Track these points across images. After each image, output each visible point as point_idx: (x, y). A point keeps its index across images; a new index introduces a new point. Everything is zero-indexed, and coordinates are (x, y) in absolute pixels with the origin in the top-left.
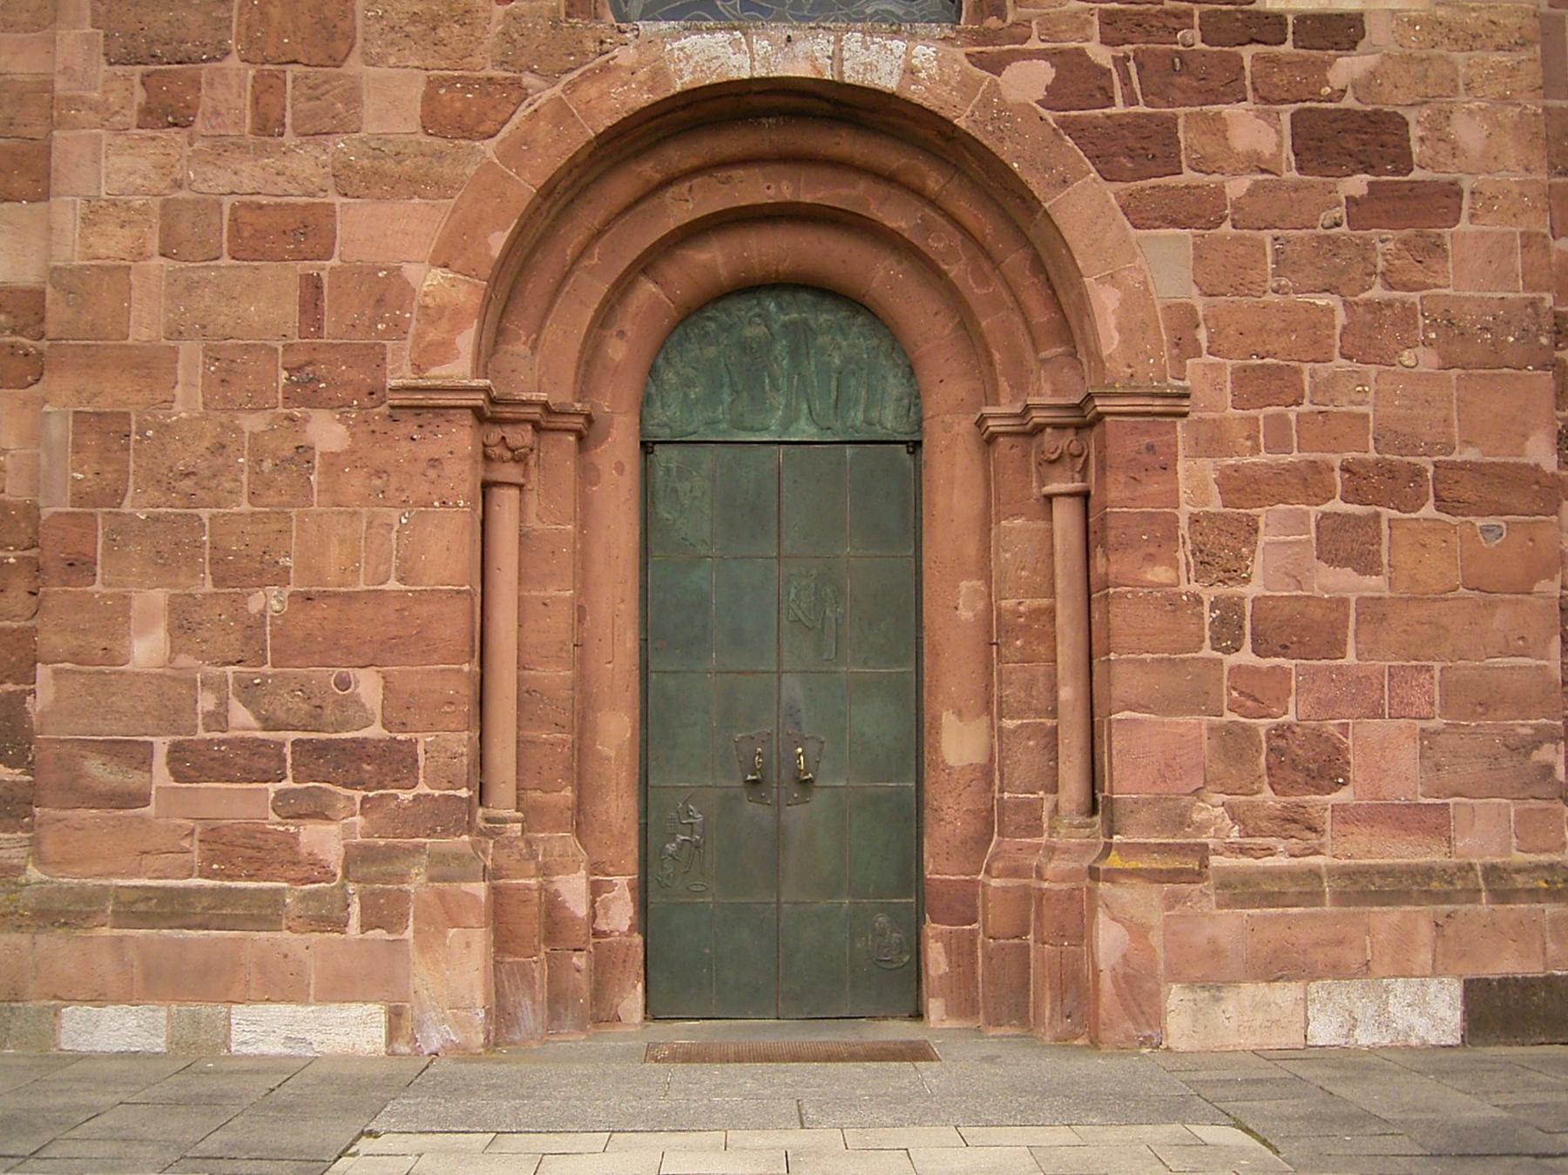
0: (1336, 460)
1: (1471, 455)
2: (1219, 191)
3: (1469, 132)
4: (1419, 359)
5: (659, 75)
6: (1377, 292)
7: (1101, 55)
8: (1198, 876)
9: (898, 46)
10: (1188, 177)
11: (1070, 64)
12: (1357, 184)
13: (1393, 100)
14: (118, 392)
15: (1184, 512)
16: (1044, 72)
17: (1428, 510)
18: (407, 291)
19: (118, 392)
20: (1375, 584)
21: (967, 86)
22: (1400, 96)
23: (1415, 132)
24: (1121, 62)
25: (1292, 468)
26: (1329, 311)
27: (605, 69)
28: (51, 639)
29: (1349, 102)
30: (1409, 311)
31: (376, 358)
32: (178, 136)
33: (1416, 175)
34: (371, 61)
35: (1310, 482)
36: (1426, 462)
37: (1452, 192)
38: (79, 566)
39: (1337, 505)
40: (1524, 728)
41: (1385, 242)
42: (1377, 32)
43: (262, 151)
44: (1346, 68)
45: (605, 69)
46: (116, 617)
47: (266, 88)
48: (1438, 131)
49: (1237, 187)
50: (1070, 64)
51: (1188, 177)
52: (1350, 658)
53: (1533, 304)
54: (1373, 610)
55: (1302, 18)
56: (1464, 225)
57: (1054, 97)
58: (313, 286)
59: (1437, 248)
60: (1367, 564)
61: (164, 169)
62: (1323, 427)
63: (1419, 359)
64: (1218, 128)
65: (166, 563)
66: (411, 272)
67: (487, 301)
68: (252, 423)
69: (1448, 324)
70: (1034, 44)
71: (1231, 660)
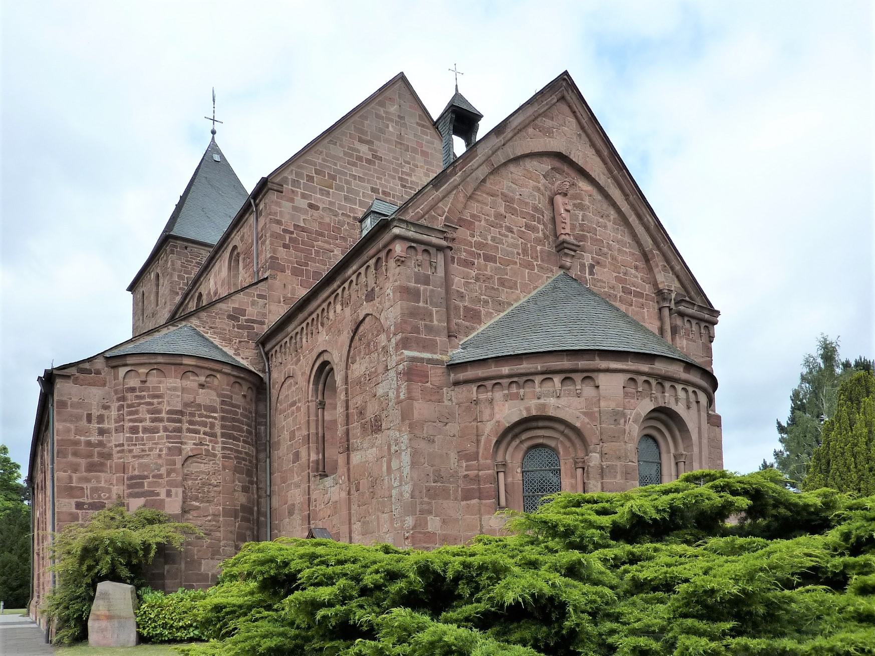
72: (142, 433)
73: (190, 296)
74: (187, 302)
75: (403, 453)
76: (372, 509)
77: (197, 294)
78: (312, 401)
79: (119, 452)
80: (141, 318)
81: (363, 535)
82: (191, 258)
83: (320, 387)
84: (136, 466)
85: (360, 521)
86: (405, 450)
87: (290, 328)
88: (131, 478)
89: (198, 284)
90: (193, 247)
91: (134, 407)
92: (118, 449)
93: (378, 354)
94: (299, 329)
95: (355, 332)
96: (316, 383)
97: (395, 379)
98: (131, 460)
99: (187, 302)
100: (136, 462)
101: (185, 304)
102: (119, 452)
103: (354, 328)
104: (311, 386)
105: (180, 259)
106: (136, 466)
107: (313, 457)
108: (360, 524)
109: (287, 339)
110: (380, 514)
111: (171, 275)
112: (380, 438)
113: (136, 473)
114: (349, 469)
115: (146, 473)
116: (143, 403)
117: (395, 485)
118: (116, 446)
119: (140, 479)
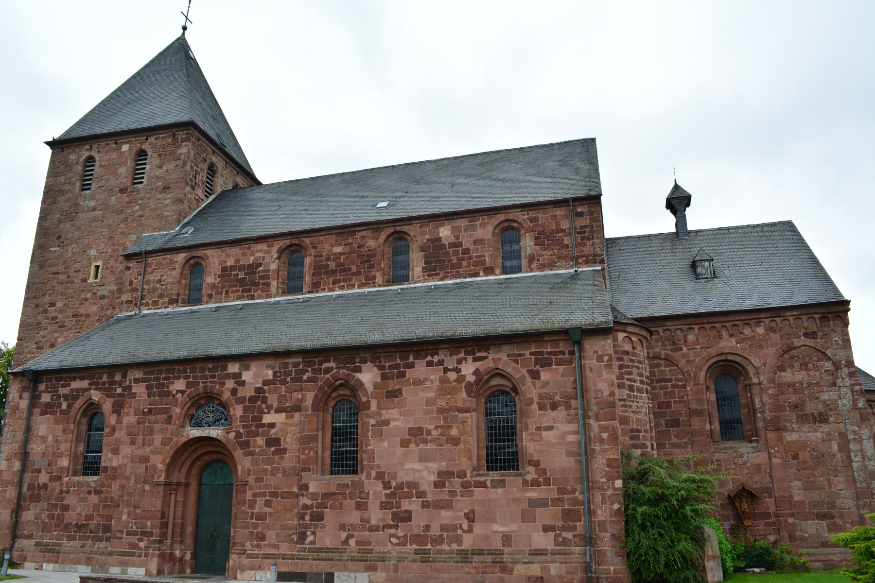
0: (267, 491)
1: (286, 490)
2: (255, 451)
3: (289, 440)
4: (280, 475)
5: (188, 436)
6: (275, 465)
7: (242, 431)
8: (244, 554)
9: (217, 431)
10: (251, 449)
11: (238, 433)
12: (273, 449)
13: (279, 435)
14: (124, 482)
15: (247, 499)
16: (234, 434)
17: (279, 499)
18: (157, 468)
19: (124, 482)
20: (271, 510)
21: (225, 436)
22: (280, 435)
23: (282, 440)
24: (244, 432)
25: (262, 492)
26: (268, 468)
27: (182, 436)
28: (114, 516)
29: (273, 436)
30: (279, 468)
31: (153, 477)
32: (133, 446)
33: (282, 447)
34: (156, 435)
35: (263, 494)
36: (280, 491)
37: (286, 449)
38: (118, 506)
39: (267, 498)
40: (290, 532)
41: (277, 457)
42: (277, 425)
43: (143, 448)
44: (273, 431)
45: (182, 436)
46: (121, 513)
47: (144, 439)
48: (284, 440)
49: (257, 450)
50: (238, 433)
51: (251, 449)
52: (267, 521)
53: (296, 466)
54: (271, 514)
55: (268, 424)
56: (287, 454)
57: (235, 438)
58: (147, 467)
59: (283, 458)
60: (270, 507)
61: (132, 451)
62: (267, 486)
63: (280, 475)
64: (255, 441)
65: (128, 505)
66: (158, 465)
67: (166, 468)
68: (139, 486)
69: (284, 470)
70: (234, 430)
71: (252, 521)
72: (637, 392)
73: (371, 227)
74: (358, 229)
75: (865, 442)
76: (819, 473)
77: (392, 230)
78: (703, 384)
79: (623, 406)
80: (78, 184)
81: (804, 490)
82: (200, 151)
83: (708, 376)
84: (634, 420)
85: (800, 480)
86: (867, 439)
87: (669, 323)
88: (632, 431)
89: (404, 223)
90: (205, 143)
91: (629, 368)
92: (622, 403)
93: (821, 374)
94: (684, 327)
95: (785, 352)
96: (707, 373)
97: (850, 394)
98: (631, 414)
99: (358, 229)
100: (634, 417)
101: (352, 229)
102: (623, 406)
103: (785, 348)
104: (703, 373)
105: (194, 150)
106: (634, 420)
107: (708, 427)
108: (800, 482)
109: (660, 330)
110: (832, 478)
111: (184, 164)
112: (825, 428)
113: (635, 426)
114: (782, 444)
115: (640, 427)
116: (634, 366)
117: (856, 460)
118: (620, 400)
119: (638, 432)
